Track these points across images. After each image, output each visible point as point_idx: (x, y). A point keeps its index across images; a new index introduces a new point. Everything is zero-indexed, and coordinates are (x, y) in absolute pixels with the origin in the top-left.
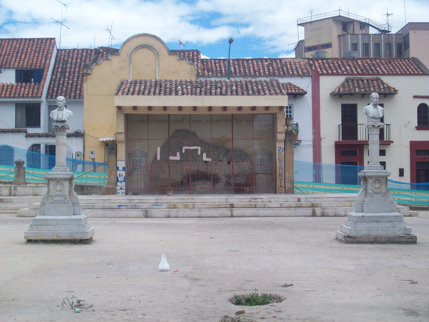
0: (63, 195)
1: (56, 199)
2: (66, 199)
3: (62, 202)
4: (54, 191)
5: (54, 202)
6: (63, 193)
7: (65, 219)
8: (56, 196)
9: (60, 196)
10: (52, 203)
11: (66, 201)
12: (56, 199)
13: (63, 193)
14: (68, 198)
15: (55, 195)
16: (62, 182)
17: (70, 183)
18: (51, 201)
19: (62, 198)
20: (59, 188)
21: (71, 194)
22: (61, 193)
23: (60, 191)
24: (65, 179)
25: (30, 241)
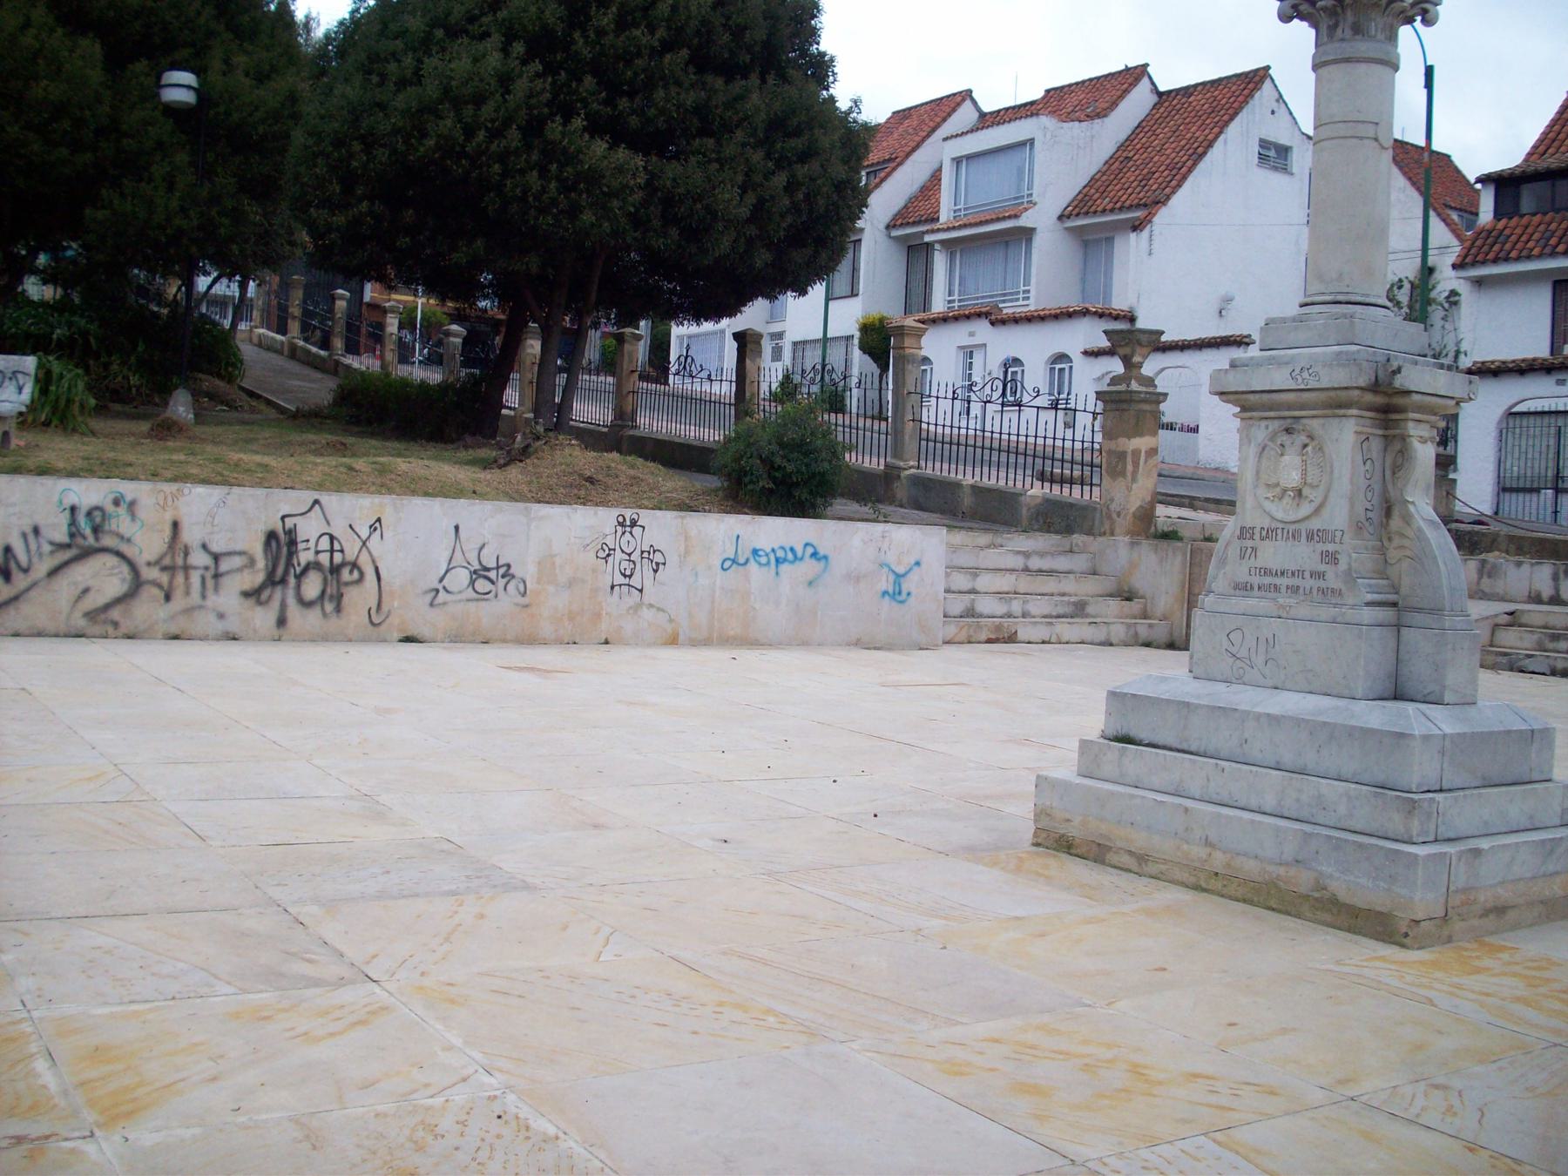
0: (1315, 524)
1: (1273, 554)
2: (1331, 558)
3: (1309, 583)
4: (1262, 492)
5: (1256, 580)
6: (1317, 511)
7: (1298, 722)
8: (1269, 534)
9: (1295, 536)
10: (1244, 588)
11: (1332, 581)
12: (1273, 554)
13: (1317, 511)
14: (1355, 553)
15: (1266, 523)
16: (1315, 424)
17: (1387, 440)
18: (1242, 575)
19: (1303, 555)
20: (1290, 470)
21: (1396, 523)
22: (1306, 509)
23: (1299, 493)
24: (1335, 403)
25: (1057, 841)
